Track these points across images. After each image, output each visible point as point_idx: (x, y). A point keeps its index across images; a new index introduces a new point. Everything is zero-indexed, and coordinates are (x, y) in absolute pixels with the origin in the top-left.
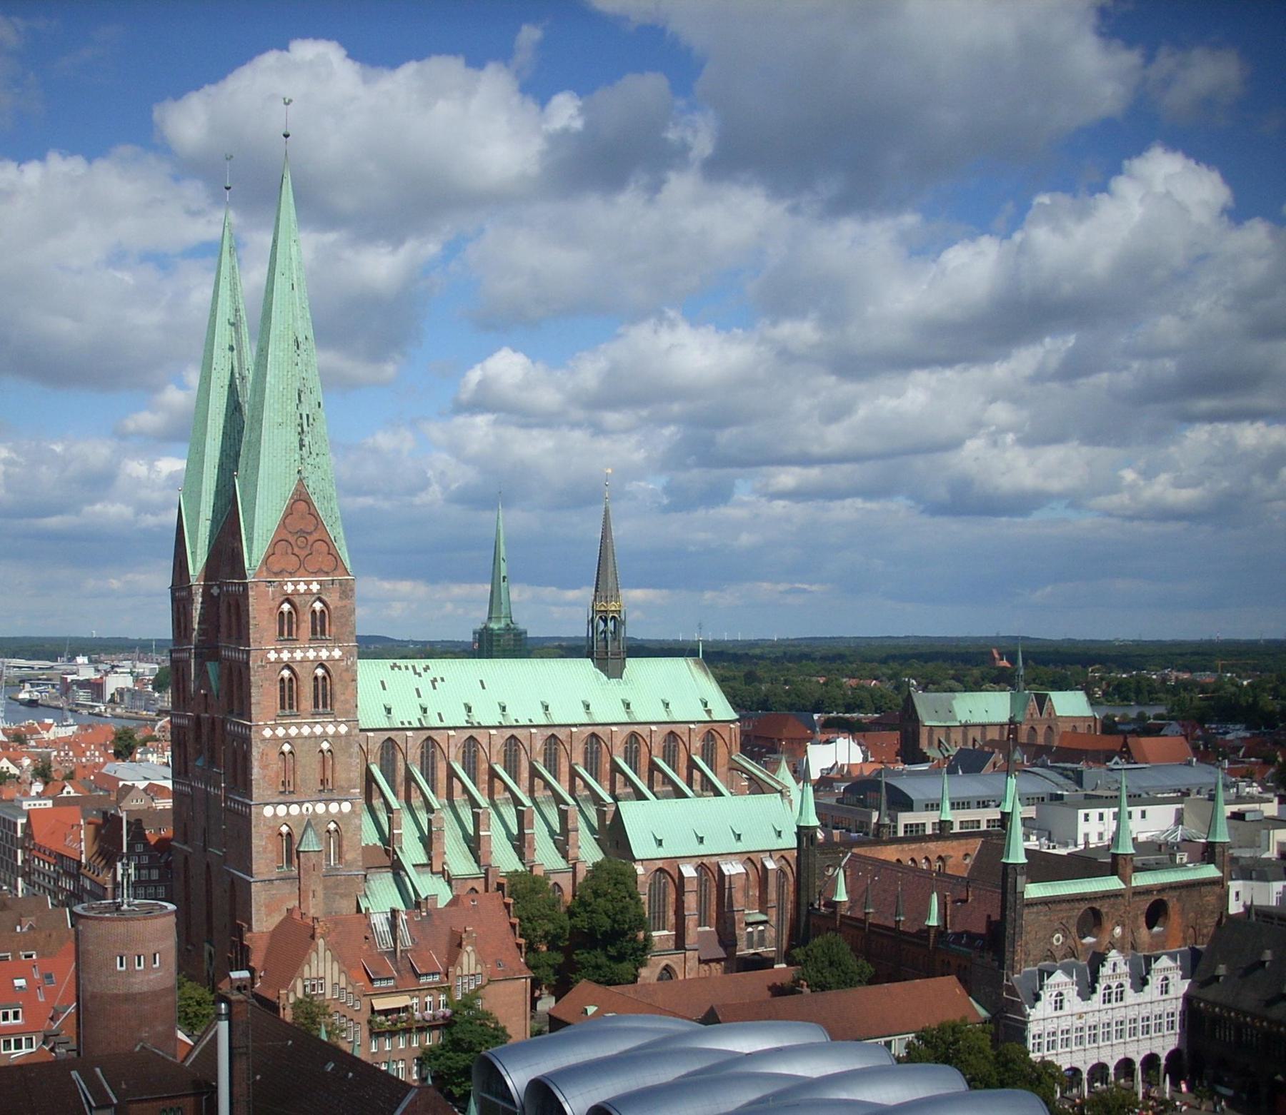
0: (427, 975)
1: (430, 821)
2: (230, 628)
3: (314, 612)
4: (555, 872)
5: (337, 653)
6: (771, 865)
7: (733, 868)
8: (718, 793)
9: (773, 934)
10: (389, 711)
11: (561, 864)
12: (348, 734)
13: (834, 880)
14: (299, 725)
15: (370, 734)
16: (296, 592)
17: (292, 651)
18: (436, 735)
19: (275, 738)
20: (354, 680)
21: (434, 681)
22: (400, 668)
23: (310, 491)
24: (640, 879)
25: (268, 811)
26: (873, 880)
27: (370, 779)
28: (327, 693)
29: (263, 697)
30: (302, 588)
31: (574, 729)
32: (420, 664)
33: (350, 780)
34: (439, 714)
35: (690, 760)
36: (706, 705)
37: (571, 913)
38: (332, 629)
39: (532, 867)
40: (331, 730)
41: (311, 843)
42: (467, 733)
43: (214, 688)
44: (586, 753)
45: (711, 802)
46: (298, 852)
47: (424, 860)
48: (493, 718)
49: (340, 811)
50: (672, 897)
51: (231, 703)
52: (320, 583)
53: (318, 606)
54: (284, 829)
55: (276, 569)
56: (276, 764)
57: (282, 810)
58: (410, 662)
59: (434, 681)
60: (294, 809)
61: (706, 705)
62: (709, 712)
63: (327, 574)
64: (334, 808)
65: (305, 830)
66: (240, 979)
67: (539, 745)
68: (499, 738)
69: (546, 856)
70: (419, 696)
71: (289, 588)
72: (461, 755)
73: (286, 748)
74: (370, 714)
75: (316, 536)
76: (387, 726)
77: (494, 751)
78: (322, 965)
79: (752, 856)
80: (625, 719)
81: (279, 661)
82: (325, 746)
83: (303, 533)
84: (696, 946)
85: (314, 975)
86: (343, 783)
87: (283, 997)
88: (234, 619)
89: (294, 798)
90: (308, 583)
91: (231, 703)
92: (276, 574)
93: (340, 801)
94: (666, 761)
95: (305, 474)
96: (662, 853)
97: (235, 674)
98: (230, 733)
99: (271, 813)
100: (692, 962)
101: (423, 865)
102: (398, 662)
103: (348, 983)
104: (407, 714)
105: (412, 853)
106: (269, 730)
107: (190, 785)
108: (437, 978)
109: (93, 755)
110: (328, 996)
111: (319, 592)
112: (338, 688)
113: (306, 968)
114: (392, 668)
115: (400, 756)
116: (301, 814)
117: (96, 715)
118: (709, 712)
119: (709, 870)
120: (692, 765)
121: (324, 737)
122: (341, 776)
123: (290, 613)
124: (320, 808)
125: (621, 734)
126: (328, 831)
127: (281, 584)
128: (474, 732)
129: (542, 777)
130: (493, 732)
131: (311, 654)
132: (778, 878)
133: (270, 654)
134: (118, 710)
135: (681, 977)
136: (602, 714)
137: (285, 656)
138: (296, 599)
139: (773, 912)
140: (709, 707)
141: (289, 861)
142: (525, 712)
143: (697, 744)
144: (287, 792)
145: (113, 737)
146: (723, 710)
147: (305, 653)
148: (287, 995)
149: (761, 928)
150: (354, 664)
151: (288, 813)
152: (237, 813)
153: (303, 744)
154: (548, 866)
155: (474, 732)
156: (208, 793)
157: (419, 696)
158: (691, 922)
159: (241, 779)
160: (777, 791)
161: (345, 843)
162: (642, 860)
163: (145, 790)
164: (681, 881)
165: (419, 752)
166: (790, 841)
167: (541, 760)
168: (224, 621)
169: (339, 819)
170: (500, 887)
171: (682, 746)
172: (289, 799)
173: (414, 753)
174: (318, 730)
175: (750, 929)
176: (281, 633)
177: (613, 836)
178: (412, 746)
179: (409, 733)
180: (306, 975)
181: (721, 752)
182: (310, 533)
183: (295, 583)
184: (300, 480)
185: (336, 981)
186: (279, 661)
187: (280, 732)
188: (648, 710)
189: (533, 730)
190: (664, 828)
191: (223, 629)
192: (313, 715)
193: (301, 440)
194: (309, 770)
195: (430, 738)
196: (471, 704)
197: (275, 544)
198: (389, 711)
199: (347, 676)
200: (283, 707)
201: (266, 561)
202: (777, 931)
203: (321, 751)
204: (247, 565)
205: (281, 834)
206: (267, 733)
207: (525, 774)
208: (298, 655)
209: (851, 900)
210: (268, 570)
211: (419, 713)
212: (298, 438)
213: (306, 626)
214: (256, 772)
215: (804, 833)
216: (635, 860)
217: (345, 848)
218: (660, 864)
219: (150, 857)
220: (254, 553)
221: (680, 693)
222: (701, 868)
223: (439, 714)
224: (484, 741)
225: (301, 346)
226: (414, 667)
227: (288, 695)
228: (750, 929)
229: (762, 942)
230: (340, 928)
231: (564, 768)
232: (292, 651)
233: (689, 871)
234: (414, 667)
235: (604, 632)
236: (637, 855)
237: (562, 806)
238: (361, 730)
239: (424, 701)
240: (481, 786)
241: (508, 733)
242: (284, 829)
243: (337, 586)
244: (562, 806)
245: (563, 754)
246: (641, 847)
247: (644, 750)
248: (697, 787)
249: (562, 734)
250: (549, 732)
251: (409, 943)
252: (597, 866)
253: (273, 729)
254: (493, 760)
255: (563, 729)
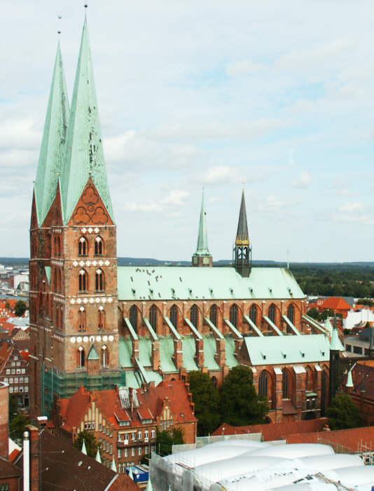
0: (146, 420)
1: (153, 345)
2: (55, 249)
3: (96, 243)
4: (213, 371)
5: (107, 263)
6: (319, 369)
7: (300, 370)
8: (294, 334)
9: (319, 402)
10: (134, 292)
11: (216, 367)
12: (112, 303)
13: (347, 375)
14: (88, 298)
15: (125, 303)
16: (87, 233)
17: (85, 261)
18: (158, 304)
19: (76, 304)
20: (116, 276)
21: (157, 278)
22: (140, 271)
23: (95, 183)
24: (255, 375)
25: (73, 340)
26: (365, 377)
27: (123, 325)
28: (101, 283)
29: (71, 283)
30: (90, 230)
31: (225, 302)
32: (150, 269)
33: (113, 325)
34: (159, 294)
35: (281, 317)
36: (290, 291)
37: (221, 390)
38: (105, 251)
39: (202, 368)
40: (104, 300)
41: (94, 356)
42: (172, 304)
43: (49, 281)
44: (231, 313)
45: (291, 337)
46: (88, 360)
47: (149, 365)
48: (186, 296)
49: (108, 341)
50: (269, 384)
51: (56, 287)
52: (99, 228)
53: (98, 240)
54: (81, 349)
55: (78, 221)
56: (76, 317)
57: (79, 340)
58: (145, 268)
59: (157, 278)
60: (86, 339)
61: (290, 291)
62: (291, 294)
63: (103, 224)
64: (105, 338)
65: (90, 350)
66: (43, 421)
67: (207, 309)
68: (188, 306)
69: (210, 365)
70: (149, 284)
71: (84, 231)
72: (169, 313)
73: (82, 309)
74: (124, 293)
75: (98, 205)
76: (133, 299)
77: (185, 312)
78: (93, 415)
79: (310, 365)
80: (251, 297)
81: (79, 266)
82: (101, 308)
83: (91, 203)
84: (281, 408)
85: (90, 420)
86: (109, 327)
87: (74, 431)
88: (57, 245)
89: (86, 333)
90: (93, 228)
91: (56, 287)
92: (78, 224)
93: (108, 335)
94: (270, 317)
95: (92, 175)
96: (265, 362)
97: (58, 272)
98: (55, 302)
99: (75, 341)
100: (279, 416)
101: (149, 367)
102: (140, 268)
103: (107, 424)
104: (143, 293)
105: (143, 362)
106: (73, 301)
107: (38, 328)
108: (151, 422)
109: (4, 314)
110: (97, 430)
111: (99, 233)
112: (108, 280)
113: (86, 417)
114: (137, 271)
115: (139, 314)
116: (89, 342)
117: (10, 295)
118: (291, 294)
119: (288, 371)
120: (283, 320)
121: (101, 304)
122: (108, 322)
123: (84, 243)
124: (99, 339)
125: (248, 305)
126: (102, 350)
127: (80, 229)
128: (176, 303)
129: (208, 325)
130: (185, 303)
131: (95, 263)
132: (322, 376)
133: (74, 262)
134: (21, 293)
135: (274, 422)
136: (239, 295)
137: (82, 264)
138: (88, 236)
139: (320, 392)
140: (291, 292)
141: (83, 364)
142: (201, 293)
143: (285, 310)
144: (82, 328)
145: (15, 305)
146: (298, 293)
147: (92, 263)
148: (76, 429)
149: (314, 399)
150: (116, 268)
151: (83, 341)
152: (58, 341)
153: (90, 307)
154: (209, 369)
155: (176, 303)
156: (45, 331)
157: (149, 284)
158: (279, 397)
159: (59, 323)
160: (323, 333)
161: (110, 356)
162: (256, 366)
163: (26, 331)
164: (274, 375)
165: (149, 311)
166: (327, 358)
167: (208, 316)
168: (53, 247)
169: (108, 344)
170: (184, 377)
171: (277, 311)
172: (83, 334)
173: (146, 312)
174: (98, 300)
175: (308, 400)
176: (80, 253)
177: (242, 353)
178: (146, 308)
179: (144, 303)
180: (86, 420)
181: (297, 315)
182: (94, 204)
183: (87, 228)
184: (90, 178)
185: (100, 422)
186: (79, 266)
187: (79, 301)
188: (261, 293)
189: (205, 302)
190: (267, 351)
191: (53, 251)
192: (97, 293)
193: (91, 158)
194: (93, 320)
195: (154, 306)
196: (175, 289)
197: (77, 208)
198: (134, 292)
199: (112, 274)
200: (80, 289)
201: (73, 217)
202: (322, 401)
203: (99, 311)
204: (63, 219)
205: (79, 351)
206: (73, 301)
207: (200, 323)
208: (88, 263)
209: (354, 386)
210: (74, 222)
211: (149, 293)
212: (89, 157)
213: (92, 250)
214: (66, 321)
215: (333, 353)
216: (252, 366)
217: (110, 358)
218: (264, 368)
219: (22, 363)
220: (67, 213)
221: (279, 286)
222: (284, 370)
223: (159, 294)
224: (180, 307)
225: (92, 112)
226: (147, 271)
227: (83, 282)
228: (308, 400)
229: (313, 406)
230: (104, 397)
231: (219, 320)
232: (85, 261)
233: (278, 371)
234: (147, 271)
235: (242, 254)
236: (253, 363)
237: (218, 339)
238: (119, 301)
239: (151, 287)
240: (179, 329)
241: (192, 303)
242: (81, 349)
243: (107, 230)
244: (218, 339)
245: (219, 314)
246: (256, 359)
247: (259, 312)
248: (285, 331)
249: (219, 304)
250: (212, 303)
251: (137, 404)
252: (233, 368)
253: (76, 299)
254: (185, 316)
255: (219, 302)
